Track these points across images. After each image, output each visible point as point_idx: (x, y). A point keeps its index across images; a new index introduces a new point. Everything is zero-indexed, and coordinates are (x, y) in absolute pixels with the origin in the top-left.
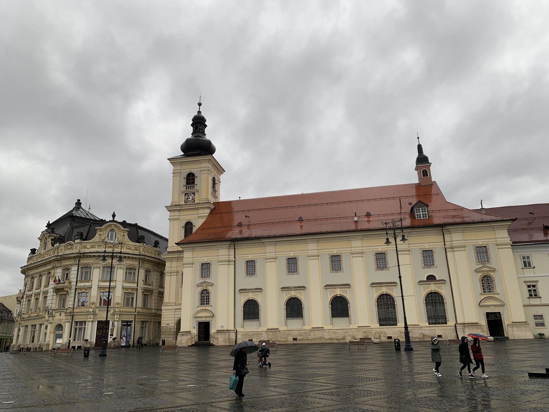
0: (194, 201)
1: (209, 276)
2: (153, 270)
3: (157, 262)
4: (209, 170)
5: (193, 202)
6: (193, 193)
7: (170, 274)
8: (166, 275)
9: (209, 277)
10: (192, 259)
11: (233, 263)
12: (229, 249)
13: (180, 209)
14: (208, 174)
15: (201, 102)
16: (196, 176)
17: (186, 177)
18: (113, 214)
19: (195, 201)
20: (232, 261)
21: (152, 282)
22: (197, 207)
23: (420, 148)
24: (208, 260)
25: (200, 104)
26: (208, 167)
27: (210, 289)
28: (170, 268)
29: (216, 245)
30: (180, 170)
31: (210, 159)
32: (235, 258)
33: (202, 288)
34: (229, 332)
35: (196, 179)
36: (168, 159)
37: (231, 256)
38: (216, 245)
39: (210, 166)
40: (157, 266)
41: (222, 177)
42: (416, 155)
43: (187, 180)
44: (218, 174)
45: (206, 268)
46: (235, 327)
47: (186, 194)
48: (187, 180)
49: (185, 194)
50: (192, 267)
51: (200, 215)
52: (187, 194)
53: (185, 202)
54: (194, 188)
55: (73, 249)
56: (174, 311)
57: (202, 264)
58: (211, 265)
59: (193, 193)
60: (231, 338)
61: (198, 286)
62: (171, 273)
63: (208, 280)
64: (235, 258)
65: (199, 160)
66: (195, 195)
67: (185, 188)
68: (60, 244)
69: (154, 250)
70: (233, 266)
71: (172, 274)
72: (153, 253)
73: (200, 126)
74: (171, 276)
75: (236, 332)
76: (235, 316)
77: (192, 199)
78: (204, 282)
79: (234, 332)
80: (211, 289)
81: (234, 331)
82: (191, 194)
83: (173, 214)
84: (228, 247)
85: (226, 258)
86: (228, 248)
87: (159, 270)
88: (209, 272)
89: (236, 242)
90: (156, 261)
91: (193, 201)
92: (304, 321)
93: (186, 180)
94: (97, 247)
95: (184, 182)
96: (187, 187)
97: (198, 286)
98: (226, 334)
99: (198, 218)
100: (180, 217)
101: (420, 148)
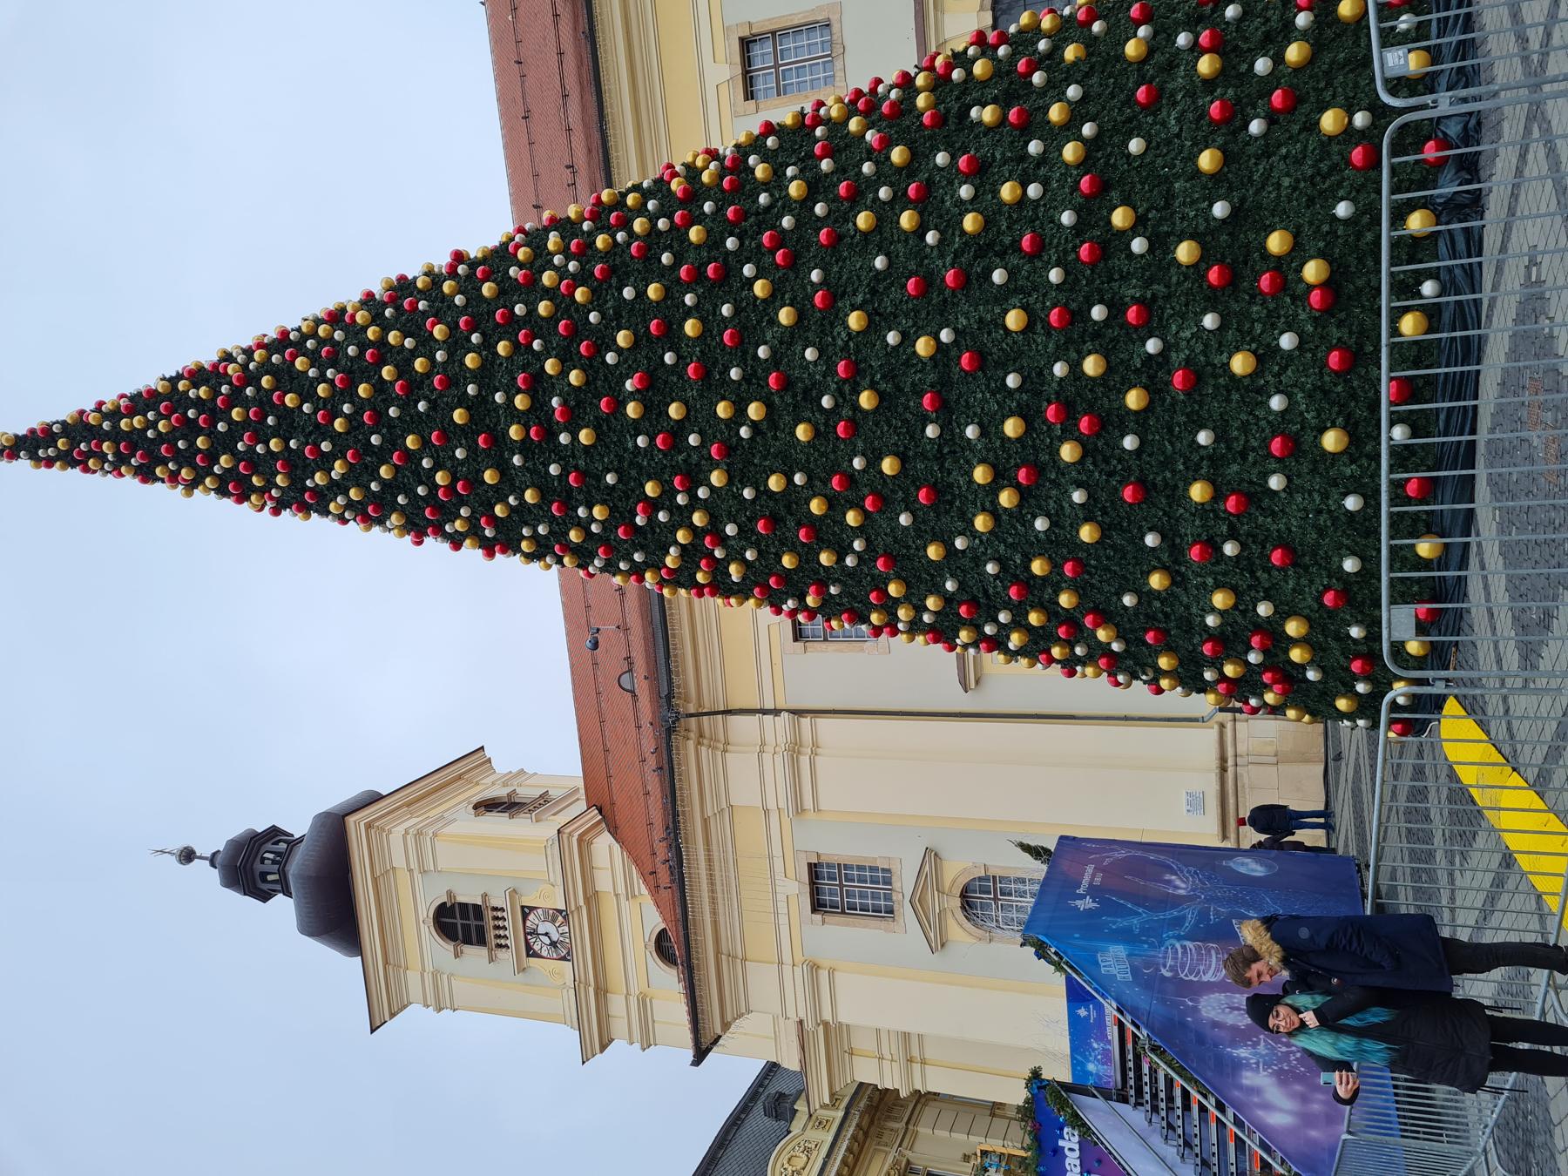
0: (560, 912)
1: (884, 870)
2: (900, 1146)
3: (865, 1124)
4: (419, 833)
6: (525, 917)
7: (917, 1067)
8: (918, 1086)
9: (889, 871)
10: (787, 969)
11: (806, 721)
12: (727, 743)
13: (591, 990)
14: (435, 835)
15: (178, 845)
16: (444, 899)
20: (797, 731)
21: (966, 1158)
22: (581, 903)
24: (791, 873)
25: (188, 856)
26: (407, 832)
27: (958, 868)
28: (886, 1064)
29: (705, 821)
31: (369, 826)
32: (776, 712)
33: (951, 923)
34: (1230, 762)
35: (461, 899)
36: (373, 1031)
37: (770, 738)
38: (705, 821)
39: (400, 830)
40: (889, 1118)
41: (503, 763)
44: (477, 784)
45: (841, 886)
46: (1195, 720)
47: (531, 952)
48: (468, 941)
49: (528, 955)
50: (831, 972)
51: (621, 890)
52: (528, 947)
53: (564, 959)
54: (502, 910)
57: (814, 910)
58: (818, 855)
59: (525, 917)
60: (1271, 749)
61: (939, 943)
62: (911, 1060)
63: (905, 882)
64: (776, 712)
65: (375, 880)
66: (532, 909)
67: (501, 954)
69: (804, 1129)
70: (823, 722)
71: (915, 1053)
72: (815, 1135)
73: (262, 863)
74: (923, 1062)
75: (1229, 715)
76: (1126, 718)
77: (553, 921)
78: (918, 903)
79: (1229, 726)
81: (1222, 726)
82: (528, 924)
83: (618, 1026)
84: (715, 748)
85: (776, 767)
86: (725, 751)
87: (910, 1108)
88: (860, 868)
89: (687, 700)
90: (854, 1124)
91: (560, 918)
93: (467, 949)
95: (475, 955)
96: (500, 946)
97: (939, 943)
98: (1245, 779)
99: (634, 896)
100: (635, 991)
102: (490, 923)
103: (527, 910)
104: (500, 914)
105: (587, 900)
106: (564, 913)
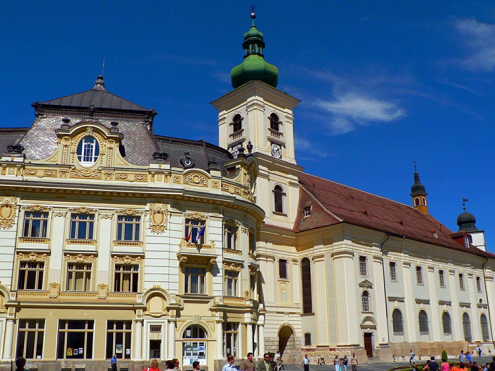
0: (281, 157)
5: (280, 158)
7: (265, 259)
23: (417, 177)
27: (369, 290)
35: (280, 125)
42: (412, 183)
55: (206, 186)
56: (275, 314)
68: (171, 167)
71: (268, 259)
80: (370, 291)
91: (280, 156)
92: (429, 336)
94: (242, 194)
101: (417, 177)
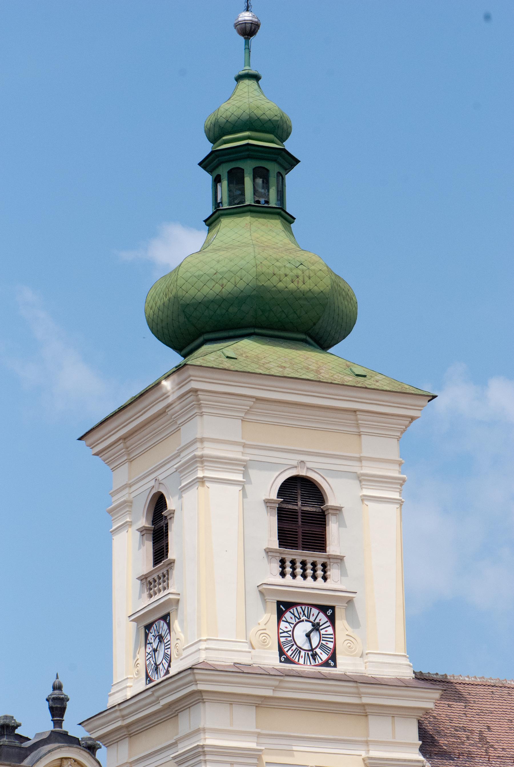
0: (333, 657)
5: (326, 664)
6: (323, 609)
13: (269, 693)
16: (332, 501)
17: (274, 495)
18: (50, 691)
19: (338, 661)
22: (365, 700)
30: (244, 446)
43: (279, 520)
49: (279, 603)
53: (281, 652)
54: (325, 578)
59: (323, 609)
66: (332, 619)
82: (315, 611)
96: (283, 562)
102: (310, 556)
103: (329, 612)
104: (320, 573)
105: (364, 705)
106: (332, 664)
